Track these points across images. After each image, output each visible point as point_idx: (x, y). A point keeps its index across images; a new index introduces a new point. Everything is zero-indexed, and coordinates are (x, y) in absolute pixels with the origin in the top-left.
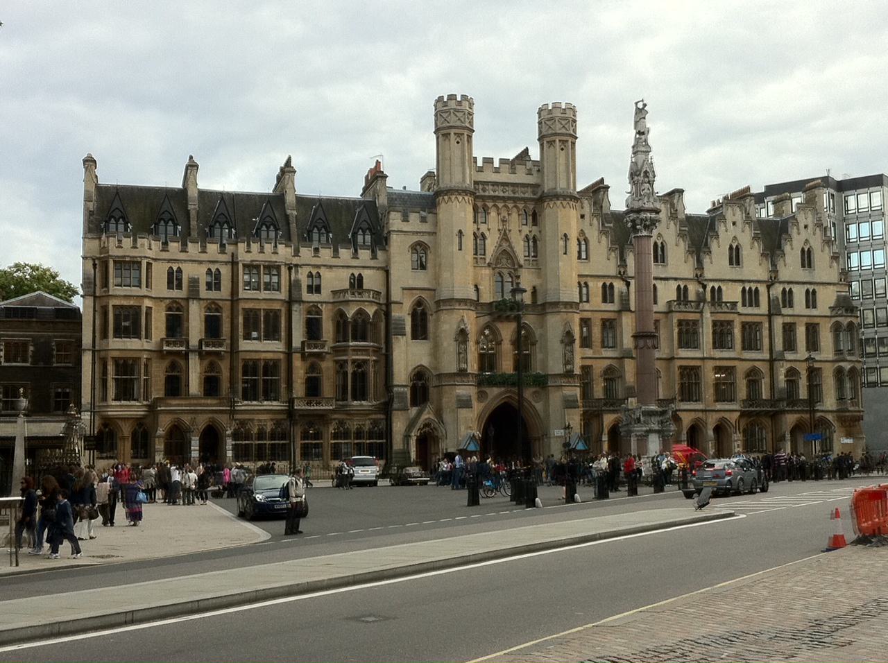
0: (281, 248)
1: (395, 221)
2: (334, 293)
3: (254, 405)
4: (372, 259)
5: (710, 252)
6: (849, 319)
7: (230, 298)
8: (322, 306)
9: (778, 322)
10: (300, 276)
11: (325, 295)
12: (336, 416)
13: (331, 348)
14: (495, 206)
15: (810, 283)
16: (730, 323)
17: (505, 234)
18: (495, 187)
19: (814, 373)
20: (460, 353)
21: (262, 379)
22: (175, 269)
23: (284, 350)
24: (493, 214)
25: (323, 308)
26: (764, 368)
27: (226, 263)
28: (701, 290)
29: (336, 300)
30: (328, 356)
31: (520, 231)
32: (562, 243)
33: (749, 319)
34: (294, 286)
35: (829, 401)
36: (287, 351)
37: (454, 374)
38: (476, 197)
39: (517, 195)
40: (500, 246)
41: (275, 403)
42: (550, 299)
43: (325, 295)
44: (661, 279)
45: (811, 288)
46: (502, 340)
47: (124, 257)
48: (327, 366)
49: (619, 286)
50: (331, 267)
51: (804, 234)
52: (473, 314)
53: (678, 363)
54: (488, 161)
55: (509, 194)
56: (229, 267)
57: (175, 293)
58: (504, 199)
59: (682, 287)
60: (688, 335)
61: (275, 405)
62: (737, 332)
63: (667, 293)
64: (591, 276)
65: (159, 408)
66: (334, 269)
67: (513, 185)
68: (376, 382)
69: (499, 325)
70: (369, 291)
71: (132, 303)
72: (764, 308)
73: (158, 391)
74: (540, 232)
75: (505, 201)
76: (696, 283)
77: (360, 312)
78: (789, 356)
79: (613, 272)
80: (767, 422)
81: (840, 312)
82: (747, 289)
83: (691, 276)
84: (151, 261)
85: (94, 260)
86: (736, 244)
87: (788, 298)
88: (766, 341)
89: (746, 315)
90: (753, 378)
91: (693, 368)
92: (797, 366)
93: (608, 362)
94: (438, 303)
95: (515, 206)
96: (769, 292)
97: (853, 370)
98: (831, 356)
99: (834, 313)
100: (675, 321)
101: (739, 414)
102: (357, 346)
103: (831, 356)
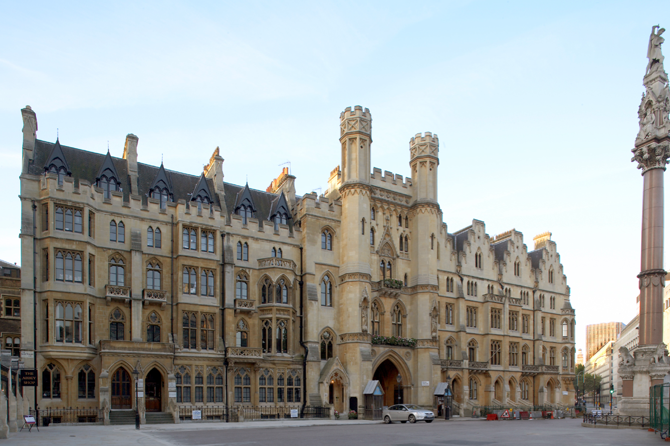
2: (260, 261)
8: (249, 271)
11: (253, 262)
13: (258, 308)
14: (382, 207)
17: (388, 230)
18: (382, 193)
21: (194, 330)
23: (219, 305)
24: (380, 214)
25: (250, 273)
28: (501, 289)
29: (262, 267)
30: (255, 314)
31: (398, 230)
36: (221, 308)
38: (373, 199)
40: (385, 239)
42: (421, 282)
45: (553, 295)
46: (385, 312)
49: (456, 279)
58: (388, 203)
59: (491, 286)
62: (520, 319)
63: (482, 288)
65: (103, 351)
66: (262, 242)
68: (294, 340)
69: (383, 300)
70: (287, 261)
72: (531, 307)
73: (102, 332)
74: (410, 232)
76: (499, 285)
77: (283, 278)
81: (567, 312)
82: (523, 292)
83: (495, 279)
88: (531, 328)
91: (515, 343)
94: (342, 278)
95: (394, 210)
96: (534, 295)
100: (490, 308)
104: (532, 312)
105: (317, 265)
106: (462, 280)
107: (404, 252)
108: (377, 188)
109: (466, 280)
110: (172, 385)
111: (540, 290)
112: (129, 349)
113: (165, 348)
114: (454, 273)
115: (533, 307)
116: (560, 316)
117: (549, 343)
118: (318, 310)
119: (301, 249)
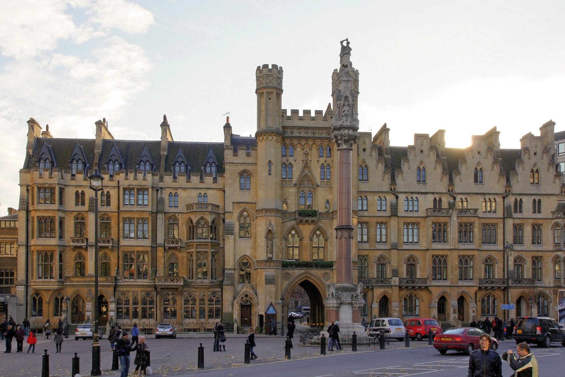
0: (149, 176)
1: (228, 155)
2: (189, 206)
3: (131, 282)
4: (214, 183)
5: (460, 173)
7: (117, 211)
9: (510, 223)
10: (164, 195)
11: (182, 208)
12: (186, 289)
15: (537, 195)
16: (471, 224)
17: (306, 163)
19: (536, 260)
20: (267, 247)
22: (80, 192)
24: (299, 149)
25: (179, 216)
27: (114, 187)
28: (452, 201)
30: (182, 249)
31: (318, 161)
33: (487, 221)
34: (160, 202)
35: (548, 280)
37: (266, 261)
39: (315, 136)
40: (303, 171)
41: (145, 280)
44: (422, 193)
48: (182, 256)
49: (390, 198)
50: (185, 189)
51: (534, 159)
52: (280, 220)
55: (310, 135)
56: (116, 189)
57: (80, 208)
59: (438, 199)
60: (440, 233)
61: (145, 282)
63: (427, 202)
64: (370, 192)
69: (301, 227)
71: (50, 214)
72: (500, 214)
73: (70, 271)
75: (307, 140)
76: (449, 196)
77: (202, 218)
78: (517, 247)
79: (386, 188)
81: (559, 215)
83: (445, 191)
84: (63, 187)
85: (28, 186)
86: (480, 167)
87: (518, 206)
89: (485, 218)
90: (489, 263)
92: (523, 255)
93: (380, 253)
96: (504, 201)
98: (551, 248)
99: (555, 216)
100: (430, 223)
101: (478, 288)
102: (199, 242)
103: (551, 248)
104: (502, 221)
105: (235, 205)
106: (397, 197)
107: (325, 180)
108: (294, 127)
109: (402, 197)
110: (112, 306)
112: (83, 282)
113: (108, 280)
114: (386, 192)
115: (502, 214)
116: (550, 221)
119: (224, 191)
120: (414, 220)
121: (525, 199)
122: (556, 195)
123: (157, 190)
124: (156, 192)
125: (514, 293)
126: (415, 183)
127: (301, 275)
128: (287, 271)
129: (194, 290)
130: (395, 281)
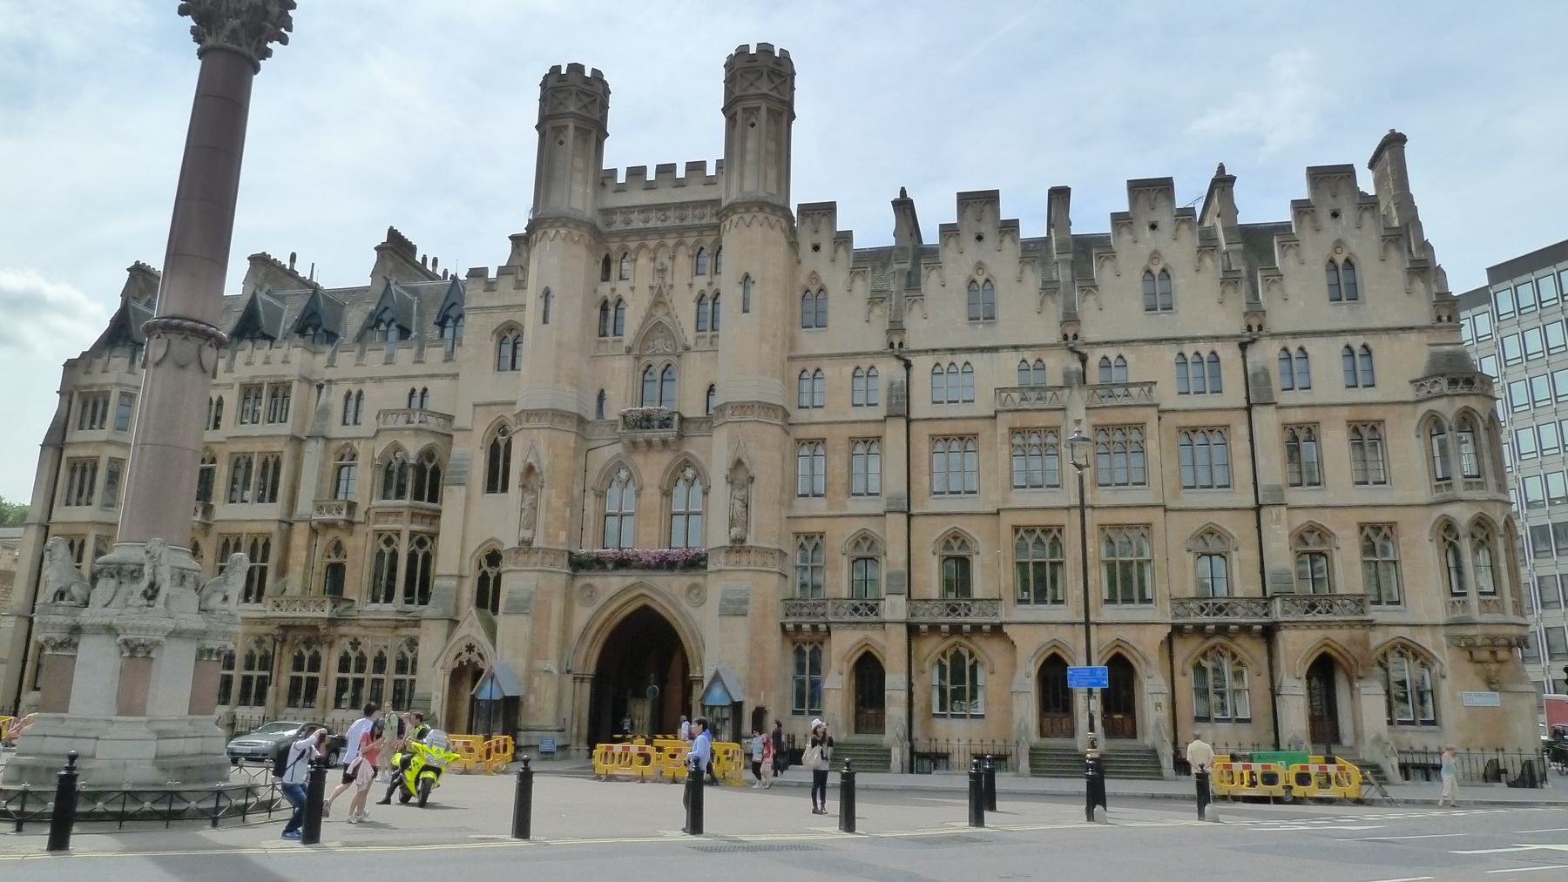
4: (445, 361)
5: (1095, 287)
6: (1460, 403)
15: (1354, 332)
16: (1140, 427)
25: (360, 448)
26: (1239, 528)
28: (1076, 365)
31: (690, 285)
32: (740, 291)
43: (368, 424)
44: (982, 350)
45: (1357, 342)
47: (91, 386)
49: (890, 370)
50: (380, 380)
53: (1008, 520)
54: (636, 173)
55: (673, 221)
58: (661, 233)
64: (831, 356)
67: (681, 206)
69: (639, 459)
72: (1234, 394)
78: (1297, 496)
79: (878, 342)
80: (1252, 650)
81: (1436, 390)
86: (1160, 267)
88: (1242, 467)
89: (1187, 411)
93: (860, 524)
96: (1244, 357)
97: (1481, 523)
99: (1423, 393)
106: (908, 365)
109: (922, 365)
111: (1273, 336)
117: (1353, 512)
118: (468, 498)
120: (960, 427)
121: (1313, 346)
122: (1421, 329)
123: (320, 387)
124: (315, 390)
125: (1298, 646)
126: (962, 320)
127: (625, 590)
128: (588, 580)
129: (363, 632)
130: (895, 608)
